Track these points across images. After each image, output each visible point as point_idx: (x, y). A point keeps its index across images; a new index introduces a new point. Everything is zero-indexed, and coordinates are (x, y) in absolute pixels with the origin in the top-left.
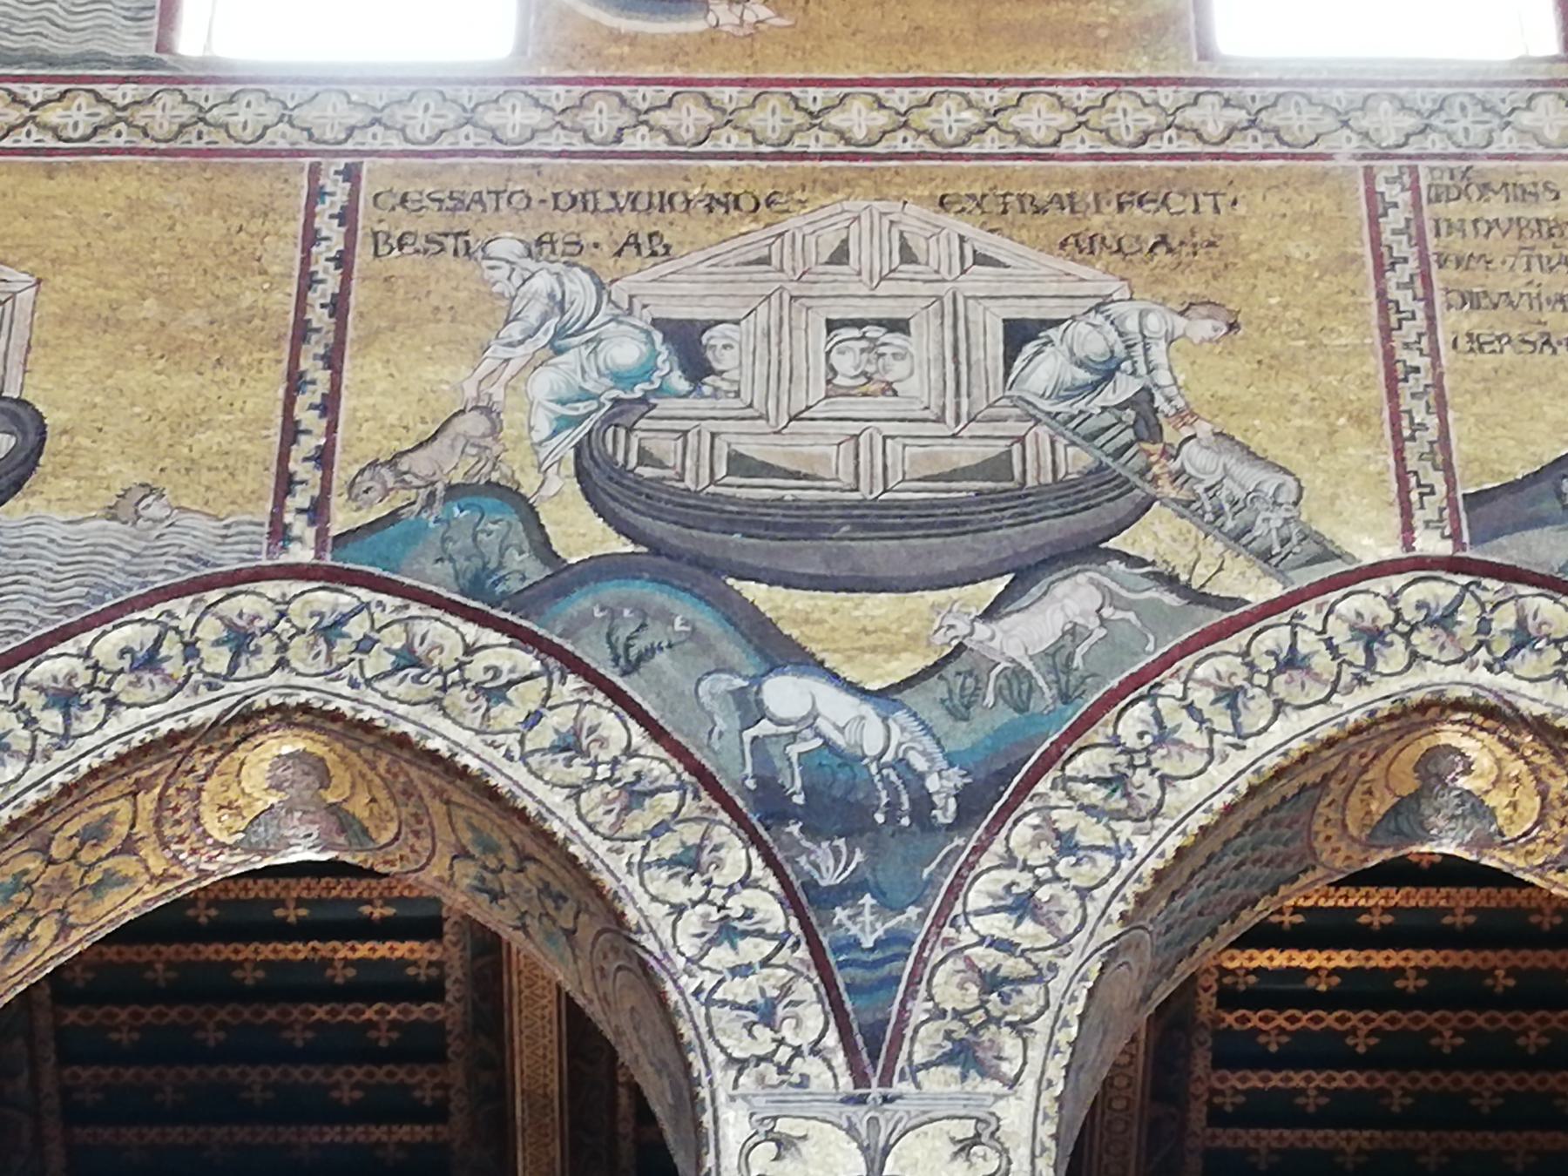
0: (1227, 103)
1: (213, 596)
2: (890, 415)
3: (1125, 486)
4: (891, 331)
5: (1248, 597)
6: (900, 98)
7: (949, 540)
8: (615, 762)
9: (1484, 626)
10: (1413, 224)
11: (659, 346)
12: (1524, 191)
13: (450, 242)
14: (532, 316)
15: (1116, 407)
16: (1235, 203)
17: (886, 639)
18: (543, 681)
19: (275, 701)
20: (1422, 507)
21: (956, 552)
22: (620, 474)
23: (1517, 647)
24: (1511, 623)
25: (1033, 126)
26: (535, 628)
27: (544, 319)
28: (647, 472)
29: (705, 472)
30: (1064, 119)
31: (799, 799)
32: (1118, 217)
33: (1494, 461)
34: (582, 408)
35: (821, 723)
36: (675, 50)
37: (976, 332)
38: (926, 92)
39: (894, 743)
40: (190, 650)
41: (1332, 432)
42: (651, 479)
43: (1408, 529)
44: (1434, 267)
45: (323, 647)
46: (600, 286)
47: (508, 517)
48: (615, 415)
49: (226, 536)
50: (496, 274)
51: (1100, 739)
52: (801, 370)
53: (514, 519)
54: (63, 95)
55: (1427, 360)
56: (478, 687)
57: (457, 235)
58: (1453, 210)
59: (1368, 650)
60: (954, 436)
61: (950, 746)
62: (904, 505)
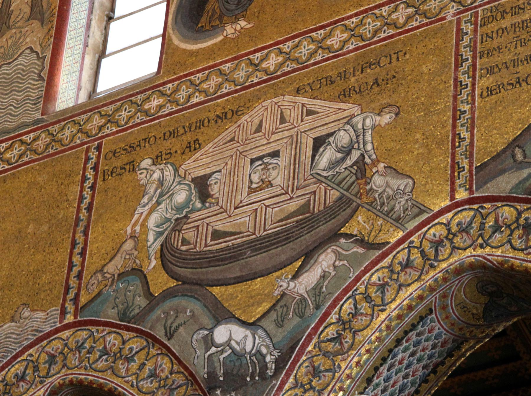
2: (267, 196)
4: (273, 157)
7: (284, 247)
8: (167, 377)
11: (193, 191)
13: (127, 167)
14: (152, 191)
15: (350, 167)
16: (405, 54)
22: (174, 251)
23: (494, 232)
26: (142, 328)
28: (184, 248)
29: (203, 242)
32: (361, 76)
35: (233, 343)
36: (211, 52)
37: (303, 147)
39: (256, 344)
40: (36, 369)
42: (185, 251)
43: (453, 190)
47: (136, 282)
49: (46, 319)
50: (143, 176)
51: (334, 320)
52: (240, 186)
58: (493, 26)
60: (292, 198)
61: (275, 340)
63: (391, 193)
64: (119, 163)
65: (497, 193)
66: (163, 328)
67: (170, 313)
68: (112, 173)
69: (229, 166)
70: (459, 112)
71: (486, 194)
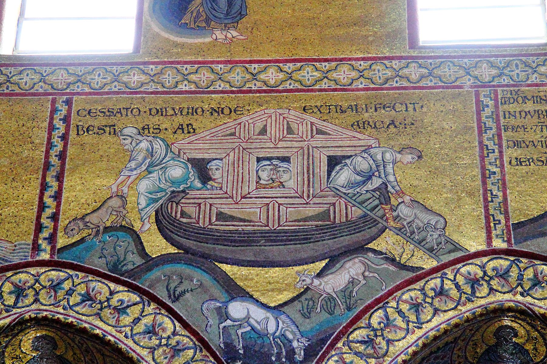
0: (420, 66)
1: (9, 274)
2: (282, 195)
3: (375, 222)
4: (282, 162)
5: (424, 267)
6: (289, 67)
7: (304, 245)
8: (169, 337)
9: (520, 277)
10: (494, 113)
11: (190, 170)
12: (541, 99)
13: (107, 129)
14: (140, 158)
15: (371, 190)
16: (422, 107)
17: (278, 286)
18: (141, 305)
19: (33, 316)
20: (496, 230)
21: (307, 250)
22: (173, 221)
23: (534, 285)
24: (531, 276)
25: (342, 77)
27: (145, 159)
28: (184, 220)
29: (207, 220)
30: (354, 74)
31: (241, 352)
32: (375, 113)
33: (525, 210)
34: (159, 195)
35: (252, 321)
36: (199, 49)
38: (299, 65)
39: (280, 328)
41: (460, 199)
44: (503, 131)
45: (53, 294)
46: (167, 146)
48: (172, 198)
49: (14, 250)
50: (126, 142)
51: (363, 325)
53: (131, 240)
55: (498, 169)
56: (115, 308)
57: (110, 126)
58: (512, 108)
59: (473, 287)
60: (307, 203)
62: (286, 232)
63: (421, 225)
64: (96, 123)
65: (538, 251)
66: (165, 290)
67: (172, 277)
68: (88, 131)
69: (231, 158)
70: (488, 172)
71: (526, 250)
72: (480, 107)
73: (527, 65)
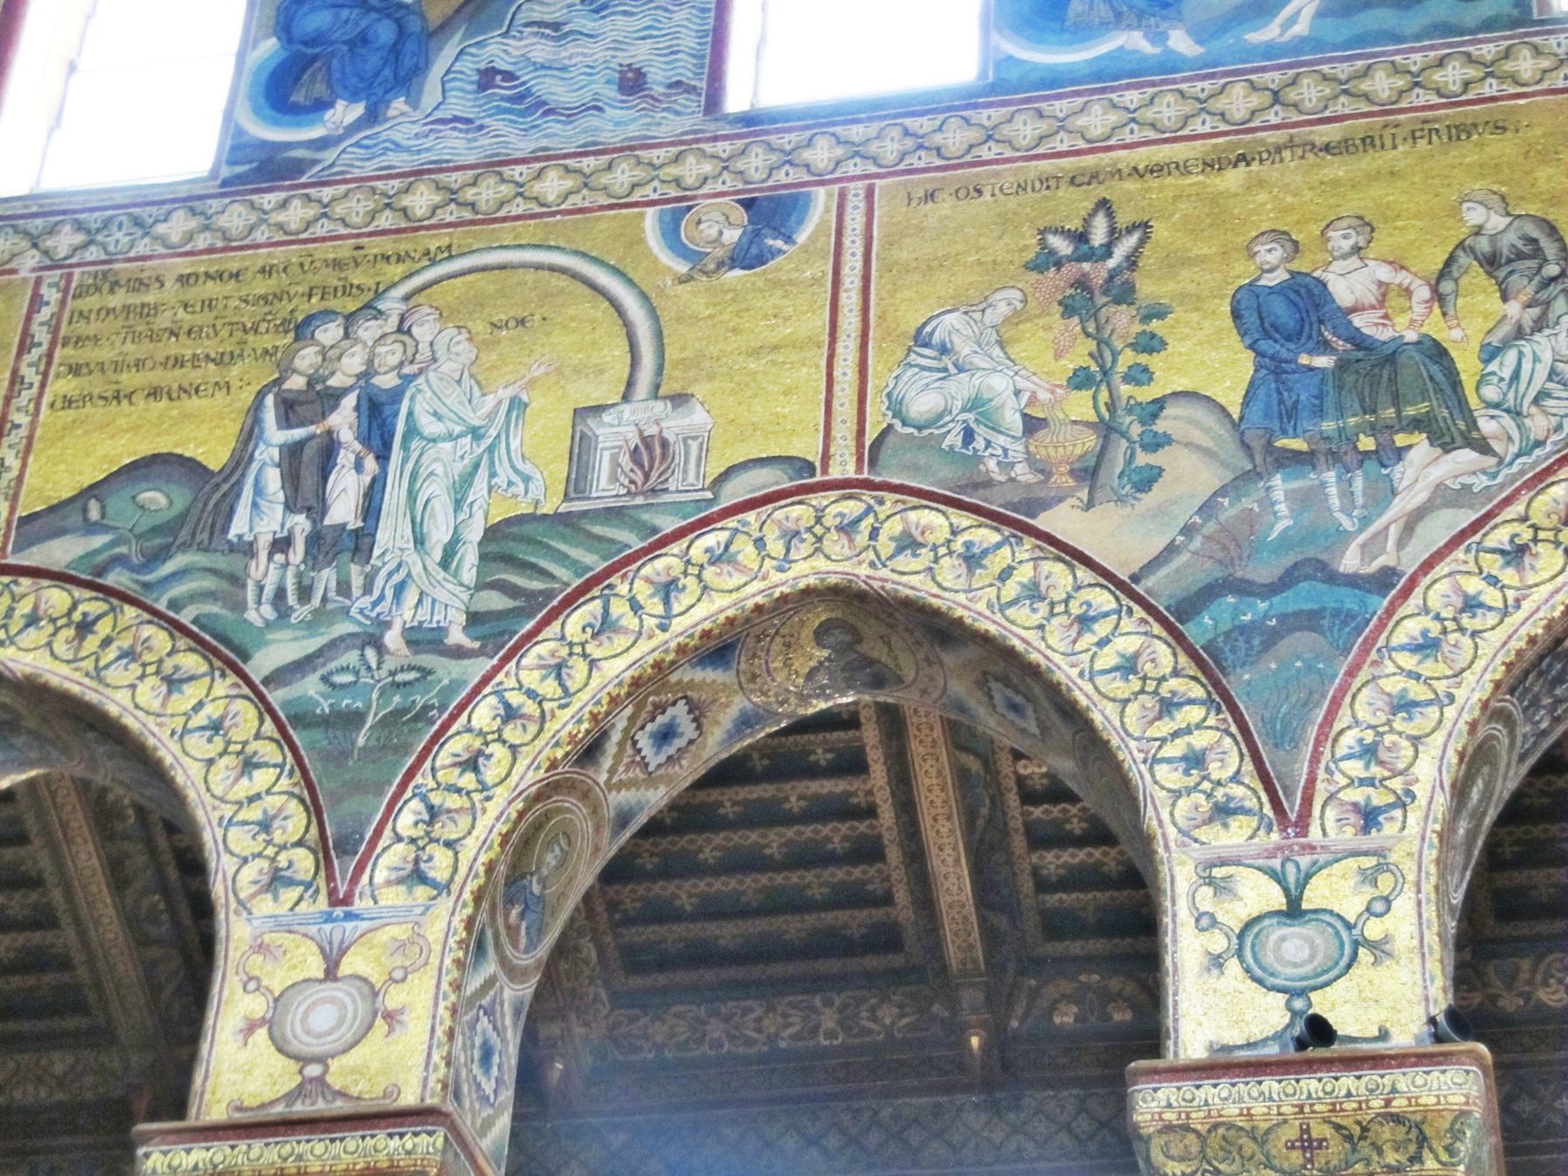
23: (27, 626)
54: (346, 195)
58: (91, 302)
72: (36, 302)
73: (138, 222)
